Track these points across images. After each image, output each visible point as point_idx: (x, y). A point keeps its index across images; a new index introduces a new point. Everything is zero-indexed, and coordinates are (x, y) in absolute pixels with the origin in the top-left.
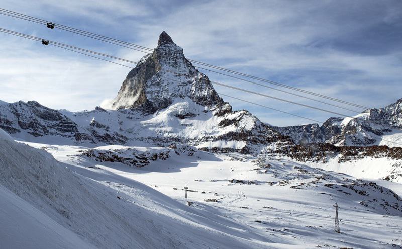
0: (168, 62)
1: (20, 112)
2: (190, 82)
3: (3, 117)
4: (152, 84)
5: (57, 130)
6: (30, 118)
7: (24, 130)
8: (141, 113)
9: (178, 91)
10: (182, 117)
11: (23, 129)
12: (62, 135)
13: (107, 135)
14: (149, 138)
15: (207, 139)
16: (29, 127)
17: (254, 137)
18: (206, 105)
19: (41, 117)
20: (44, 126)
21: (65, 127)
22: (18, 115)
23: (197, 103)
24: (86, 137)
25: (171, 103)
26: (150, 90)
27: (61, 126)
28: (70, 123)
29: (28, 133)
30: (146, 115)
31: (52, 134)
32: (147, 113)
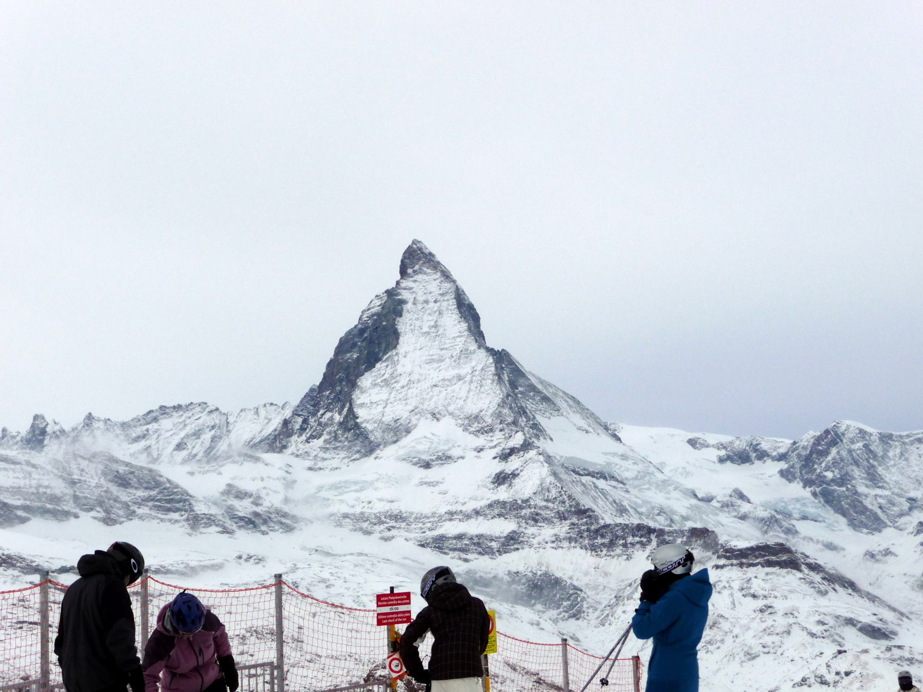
0: (418, 323)
2: (460, 378)
3: (44, 490)
4: (375, 385)
9: (430, 399)
10: (427, 465)
12: (162, 520)
13: (256, 514)
14: (346, 516)
15: (451, 515)
21: (169, 501)
23: (465, 430)
24: (210, 520)
25: (408, 431)
26: (367, 401)
27: (158, 500)
29: (95, 518)
30: (354, 460)
31: (141, 518)
32: (357, 456)
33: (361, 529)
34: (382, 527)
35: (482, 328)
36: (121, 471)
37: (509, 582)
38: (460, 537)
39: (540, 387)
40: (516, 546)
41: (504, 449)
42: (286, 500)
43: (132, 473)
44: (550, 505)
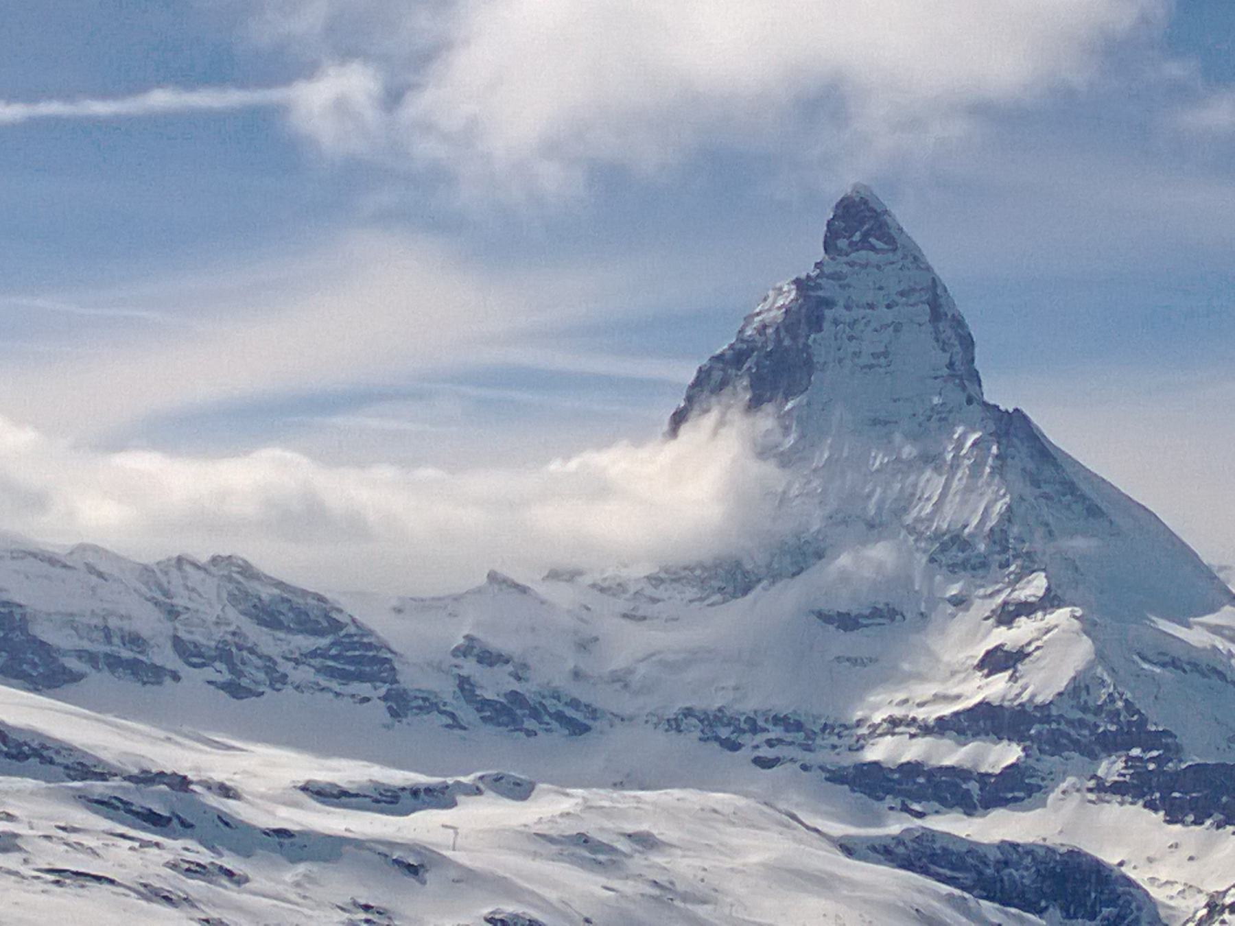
0: (852, 346)
1: (180, 602)
5: (318, 671)
6: (217, 624)
7: (196, 670)
8: (691, 592)
11: (194, 666)
12: (337, 694)
14: (688, 712)
16: (214, 659)
17: (1054, 726)
18: (965, 569)
19: (261, 622)
20: (270, 659)
22: (173, 613)
24: (430, 704)
28: (369, 646)
29: (210, 682)
32: (717, 597)
33: (717, 738)
34: (760, 738)
35: (977, 364)
36: (263, 596)
37: (998, 862)
38: (911, 769)
39: (1084, 487)
40: (1017, 794)
41: (1005, 603)
42: (577, 675)
43: (284, 600)
44: (1090, 718)
